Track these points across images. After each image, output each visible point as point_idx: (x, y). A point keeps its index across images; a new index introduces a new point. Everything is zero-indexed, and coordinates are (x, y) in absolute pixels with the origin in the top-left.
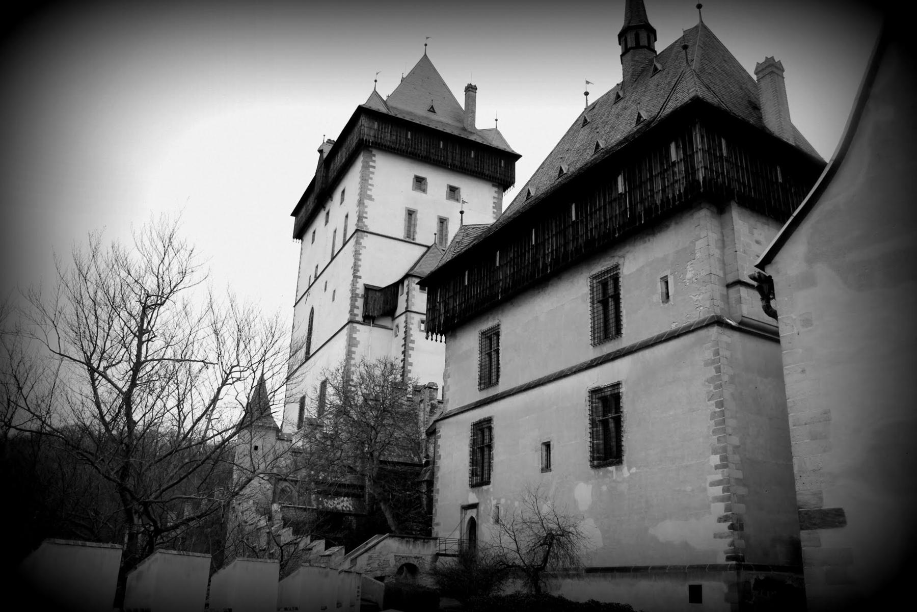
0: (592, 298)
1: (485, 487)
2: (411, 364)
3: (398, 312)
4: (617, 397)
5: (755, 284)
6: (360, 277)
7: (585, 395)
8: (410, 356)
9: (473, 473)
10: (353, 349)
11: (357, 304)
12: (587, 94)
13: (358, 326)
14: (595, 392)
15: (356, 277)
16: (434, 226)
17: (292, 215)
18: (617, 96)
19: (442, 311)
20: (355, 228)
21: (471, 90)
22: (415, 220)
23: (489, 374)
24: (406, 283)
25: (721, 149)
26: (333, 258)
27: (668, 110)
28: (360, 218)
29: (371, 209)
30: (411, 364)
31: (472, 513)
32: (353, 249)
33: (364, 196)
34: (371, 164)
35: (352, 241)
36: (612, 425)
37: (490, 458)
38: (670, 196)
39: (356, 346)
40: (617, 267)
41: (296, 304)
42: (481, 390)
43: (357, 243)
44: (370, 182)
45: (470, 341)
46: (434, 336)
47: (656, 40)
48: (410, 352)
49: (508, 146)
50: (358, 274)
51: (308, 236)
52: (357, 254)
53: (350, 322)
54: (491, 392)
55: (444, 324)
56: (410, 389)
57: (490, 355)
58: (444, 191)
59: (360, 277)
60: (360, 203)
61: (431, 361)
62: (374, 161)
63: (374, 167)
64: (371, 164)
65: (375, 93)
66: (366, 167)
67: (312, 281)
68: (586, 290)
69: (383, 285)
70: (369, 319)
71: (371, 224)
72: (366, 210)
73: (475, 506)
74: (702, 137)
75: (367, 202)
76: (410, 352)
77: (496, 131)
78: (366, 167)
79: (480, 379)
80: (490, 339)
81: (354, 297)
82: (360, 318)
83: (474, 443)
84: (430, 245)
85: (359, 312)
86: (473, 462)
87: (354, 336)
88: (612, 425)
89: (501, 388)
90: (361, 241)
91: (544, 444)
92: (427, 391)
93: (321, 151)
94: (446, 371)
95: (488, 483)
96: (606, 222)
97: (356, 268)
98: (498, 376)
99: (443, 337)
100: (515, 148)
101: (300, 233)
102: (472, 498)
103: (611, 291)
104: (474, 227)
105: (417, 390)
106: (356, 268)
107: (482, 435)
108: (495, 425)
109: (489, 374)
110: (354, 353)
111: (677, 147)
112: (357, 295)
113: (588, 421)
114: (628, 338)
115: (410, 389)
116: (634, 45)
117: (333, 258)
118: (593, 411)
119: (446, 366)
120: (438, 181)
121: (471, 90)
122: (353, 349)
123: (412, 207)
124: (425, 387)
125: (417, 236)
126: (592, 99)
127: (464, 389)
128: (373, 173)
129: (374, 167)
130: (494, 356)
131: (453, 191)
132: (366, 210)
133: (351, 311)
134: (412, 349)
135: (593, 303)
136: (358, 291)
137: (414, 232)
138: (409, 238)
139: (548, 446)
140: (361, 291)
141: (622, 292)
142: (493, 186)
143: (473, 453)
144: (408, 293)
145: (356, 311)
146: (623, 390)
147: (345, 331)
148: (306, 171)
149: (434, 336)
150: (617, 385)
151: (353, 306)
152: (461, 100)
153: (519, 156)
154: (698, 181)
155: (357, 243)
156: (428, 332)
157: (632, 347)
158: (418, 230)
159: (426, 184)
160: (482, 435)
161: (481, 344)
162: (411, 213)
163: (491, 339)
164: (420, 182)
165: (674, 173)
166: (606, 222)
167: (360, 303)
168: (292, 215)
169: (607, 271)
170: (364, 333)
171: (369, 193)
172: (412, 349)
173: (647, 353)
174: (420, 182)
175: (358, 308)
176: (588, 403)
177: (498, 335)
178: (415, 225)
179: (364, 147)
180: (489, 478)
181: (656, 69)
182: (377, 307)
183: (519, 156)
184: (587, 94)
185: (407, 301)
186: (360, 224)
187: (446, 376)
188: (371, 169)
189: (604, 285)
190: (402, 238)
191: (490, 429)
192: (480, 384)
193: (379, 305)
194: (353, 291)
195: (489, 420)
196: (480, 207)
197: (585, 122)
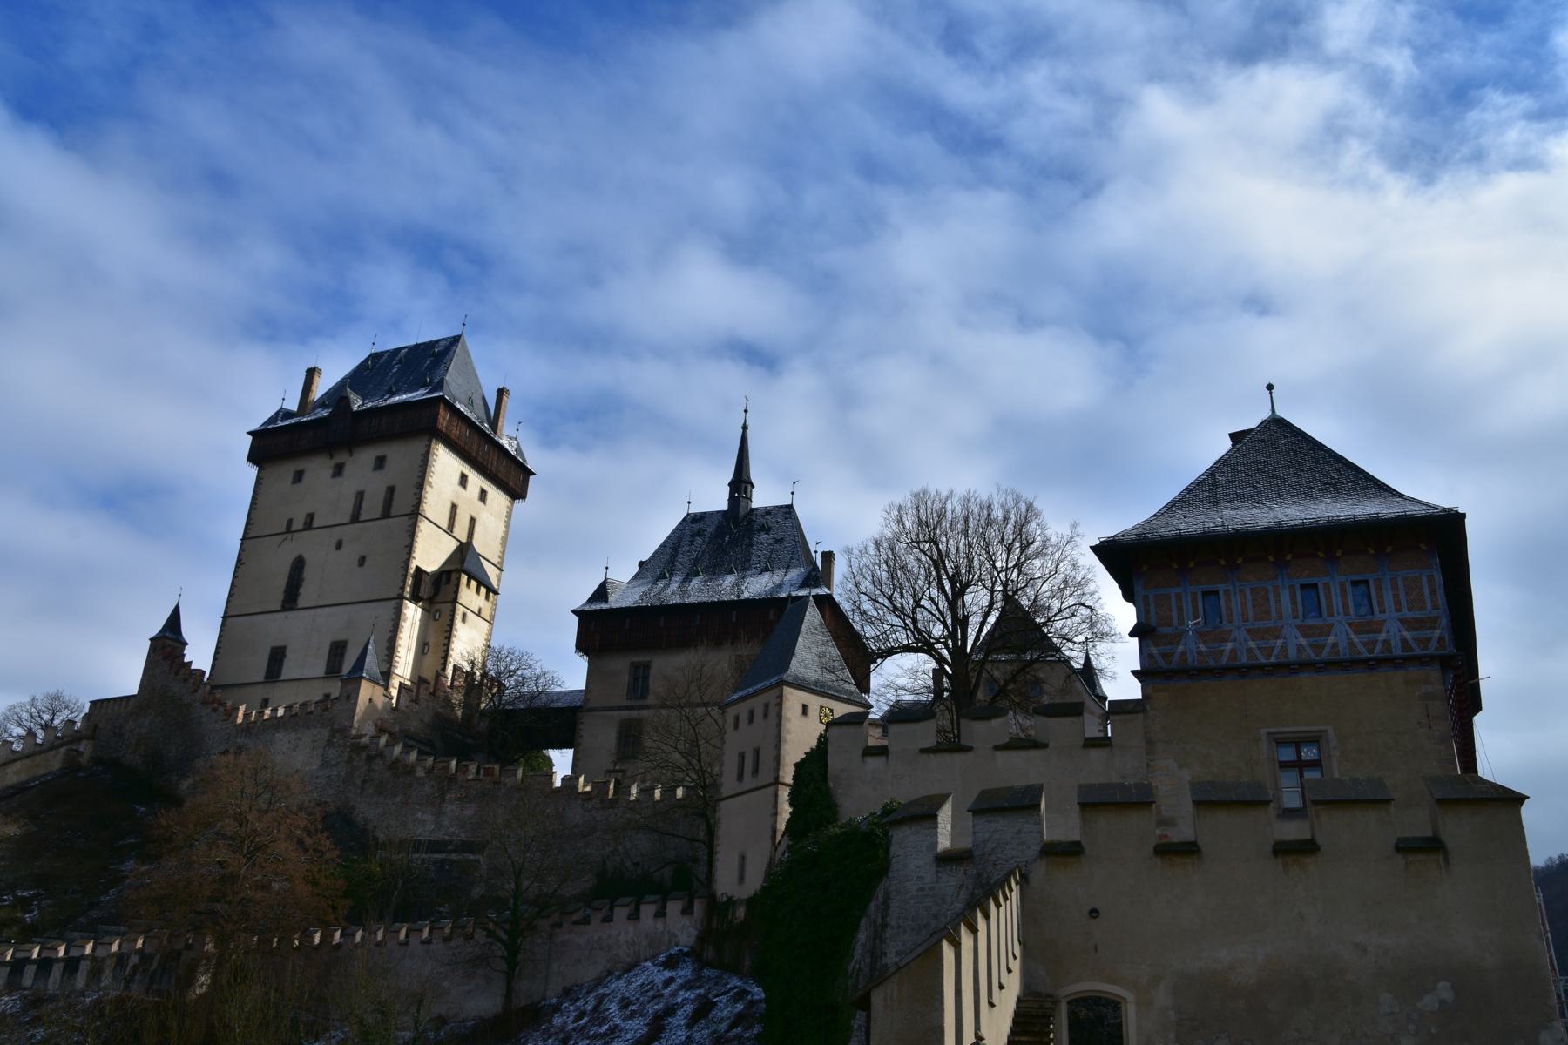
3: (439, 598)
24: (454, 576)
26: (355, 519)
58: (477, 493)
67: (298, 524)
75: (428, 488)
106: (410, 548)
120: (476, 481)
126: (696, 509)
138: (450, 529)
140: (412, 571)
155: (414, 525)
162: (454, 507)
164: (463, 480)
174: (463, 480)
179: (435, 434)
182: (425, 590)
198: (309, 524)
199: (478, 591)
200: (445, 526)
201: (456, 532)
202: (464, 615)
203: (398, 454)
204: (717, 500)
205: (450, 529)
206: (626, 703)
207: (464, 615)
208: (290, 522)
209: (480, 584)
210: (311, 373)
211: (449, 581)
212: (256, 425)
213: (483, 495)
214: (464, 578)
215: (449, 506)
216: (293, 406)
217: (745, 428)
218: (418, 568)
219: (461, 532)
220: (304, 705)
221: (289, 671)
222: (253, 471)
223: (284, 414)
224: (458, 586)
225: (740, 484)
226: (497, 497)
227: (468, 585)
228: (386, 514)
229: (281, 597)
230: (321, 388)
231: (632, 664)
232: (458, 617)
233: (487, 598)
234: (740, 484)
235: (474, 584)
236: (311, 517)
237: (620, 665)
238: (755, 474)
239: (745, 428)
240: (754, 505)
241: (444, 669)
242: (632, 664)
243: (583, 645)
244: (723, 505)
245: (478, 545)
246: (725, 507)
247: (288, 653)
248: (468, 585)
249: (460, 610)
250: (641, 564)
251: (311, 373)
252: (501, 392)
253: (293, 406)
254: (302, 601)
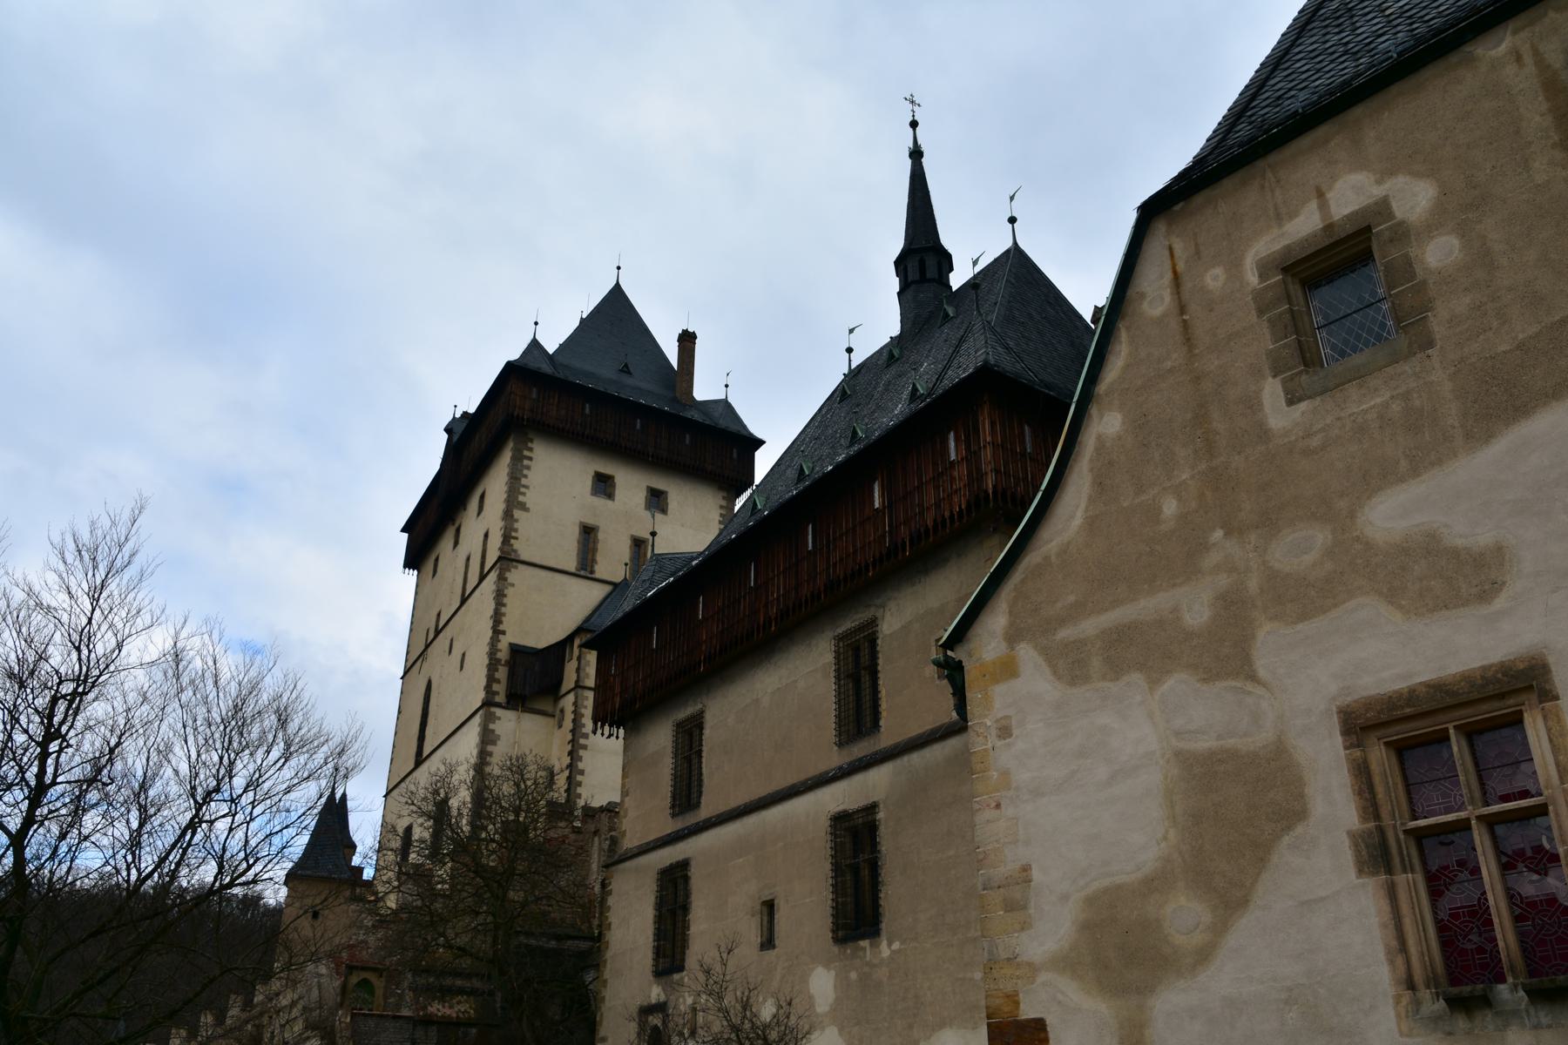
0: (837, 671)
1: (676, 977)
2: (582, 773)
3: (564, 689)
4: (873, 828)
5: (338, 796)
6: (504, 633)
7: (825, 823)
8: (580, 759)
9: (658, 953)
10: (490, 748)
11: (497, 675)
12: (849, 350)
13: (499, 712)
14: (840, 820)
15: (497, 632)
16: (624, 551)
18: (891, 355)
19: (617, 690)
20: (498, 554)
21: (687, 340)
22: (596, 541)
23: (686, 792)
25: (1023, 442)
26: (464, 600)
27: (947, 383)
28: (507, 538)
29: (523, 522)
30: (582, 773)
31: (655, 1020)
32: (494, 587)
33: (514, 503)
34: (526, 453)
35: (493, 576)
36: (865, 873)
37: (686, 927)
38: (947, 514)
39: (494, 743)
40: (873, 622)
41: (406, 673)
42: (674, 815)
43: (501, 578)
44: (524, 481)
45: (660, 738)
46: (607, 728)
47: (951, 269)
48: (581, 752)
49: (744, 427)
50: (501, 627)
52: (500, 597)
53: (487, 703)
54: (691, 819)
55: (622, 710)
56: (578, 813)
57: (689, 760)
58: (640, 497)
59: (504, 633)
60: (508, 515)
61: (604, 768)
62: (531, 450)
63: (530, 459)
64: (526, 453)
65: (535, 345)
66: (518, 459)
67: (431, 636)
68: (829, 657)
69: (542, 645)
70: (518, 700)
71: (524, 549)
72: (516, 525)
73: (660, 1008)
74: (993, 424)
75: (517, 513)
76: (581, 752)
77: (725, 405)
78: (518, 459)
79: (674, 797)
80: (691, 735)
81: (493, 665)
82: (500, 698)
83: (659, 905)
84: (618, 578)
85: (500, 688)
86: (659, 935)
87: (491, 726)
88: (865, 873)
89: (705, 811)
90: (507, 575)
91: (764, 903)
92: (604, 817)
93: (448, 430)
94: (623, 785)
95: (681, 969)
96: (855, 552)
97: (497, 618)
98: (700, 793)
99: (622, 731)
100: (756, 430)
101: (415, 558)
102: (656, 993)
103: (865, 659)
104: (672, 557)
105: (590, 813)
107: (674, 889)
108: (695, 873)
109: (686, 792)
110: (491, 754)
111: (957, 440)
112: (499, 661)
113: (828, 866)
114: (888, 737)
115: (578, 813)
116: (917, 277)
117: (464, 600)
118: (837, 850)
119: (624, 776)
121: (687, 340)
122: (490, 748)
123: (590, 521)
124: (602, 809)
125: (597, 568)
126: (858, 359)
127: (646, 817)
128: (528, 468)
129: (530, 459)
130: (695, 761)
131: (657, 500)
132: (516, 525)
133: (488, 688)
134: (585, 747)
135: (838, 678)
136: (499, 655)
137: (594, 561)
139: (770, 906)
140: (503, 655)
141: (880, 661)
142: (721, 488)
143: (659, 919)
144: (579, 659)
145: (496, 687)
146: (881, 815)
147: (477, 719)
148: (425, 460)
149: (607, 728)
150: (872, 808)
151: (491, 679)
152: (672, 353)
153: (761, 443)
154: (986, 491)
156: (595, 723)
157: (896, 746)
158: (599, 558)
159: (613, 486)
160: (674, 889)
161: (676, 742)
162: (588, 533)
163: (690, 738)
164: (604, 485)
165: (953, 479)
166: (855, 552)
167: (502, 674)
169: (860, 629)
170: (507, 723)
171: (521, 498)
172: (585, 747)
173: (915, 758)
174: (604, 485)
175: (498, 681)
176: (829, 837)
177: (701, 727)
178: (595, 550)
180: (683, 960)
181: (947, 315)
183: (761, 443)
184: (849, 350)
185: (578, 670)
186: (506, 548)
187: (625, 793)
188: (526, 462)
189: (856, 650)
190: (573, 570)
191: (686, 879)
192: (673, 807)
193: (528, 678)
194: (492, 653)
195: (684, 865)
196: (692, 525)
197: (844, 392)
200: (572, 566)
201: (601, 571)
205: (585, 568)
206: (670, 826)
215: (574, 534)
217: (916, 154)
218: (516, 650)
222: (411, 577)
228: (482, 578)
239: (916, 154)
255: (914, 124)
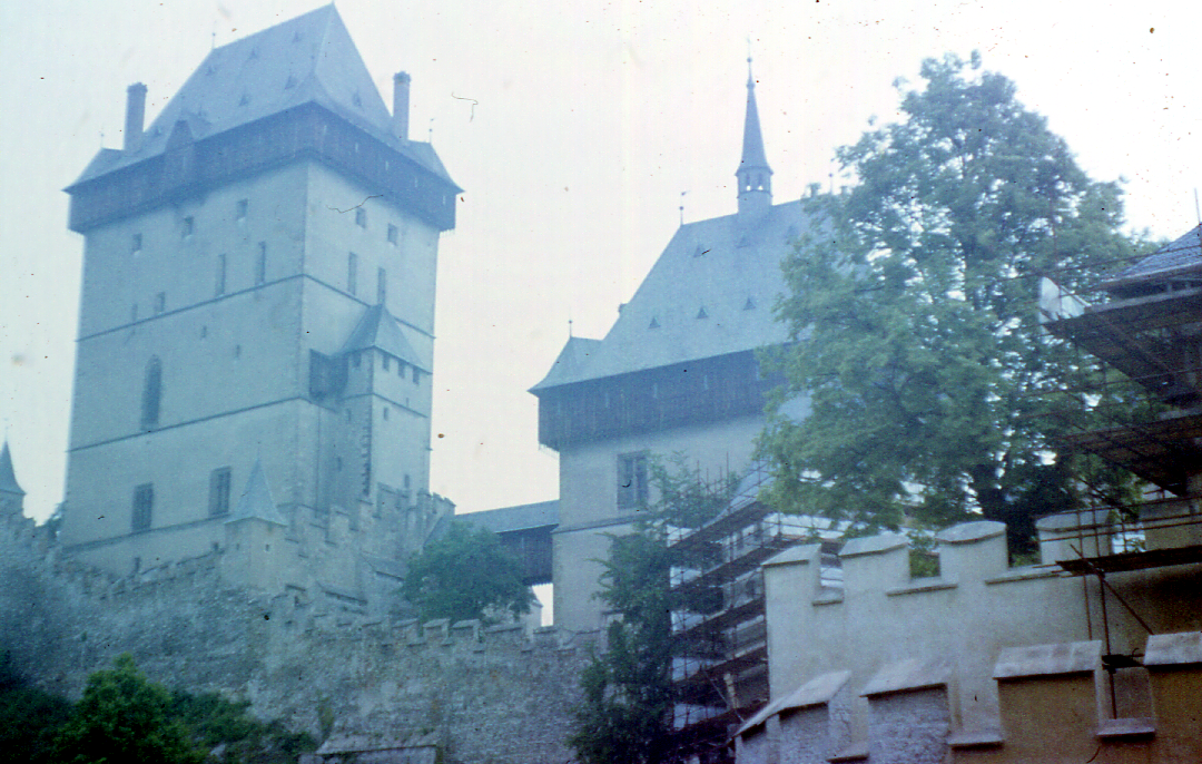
17: (66, 190)
21: (402, 80)
24: (364, 358)
51: (118, 237)
67: (146, 312)
77: (428, 147)
100: (456, 178)
120: (380, 216)
138: (350, 294)
140: (305, 354)
153: (461, 191)
164: (360, 218)
168: (66, 190)
174: (360, 218)
179: (307, 155)
183: (461, 191)
198: (161, 312)
199: (401, 373)
200: (344, 287)
202: (386, 410)
203: (266, 190)
204: (726, 203)
207: (386, 410)
208: (135, 308)
209: (402, 363)
210: (137, 93)
211: (358, 364)
212: (72, 178)
213: (391, 230)
214: (378, 362)
216: (117, 143)
217: (750, 86)
218: (314, 355)
219: (368, 291)
220: (183, 563)
221: (161, 517)
222: (78, 242)
223: (107, 155)
224: (371, 370)
225: (754, 171)
226: (414, 234)
227: (386, 367)
229: (136, 415)
230: (151, 114)
231: (620, 456)
232: (378, 419)
233: (416, 380)
234: (754, 171)
235: (394, 365)
236: (162, 297)
237: (603, 463)
238: (772, 155)
240: (775, 202)
241: (366, 492)
242: (620, 456)
243: (550, 437)
244: (730, 207)
245: (392, 307)
246: (730, 207)
247: (156, 489)
248: (386, 367)
249: (378, 406)
250: (622, 307)
251: (137, 93)
252: (402, 80)
253: (117, 143)
254: (164, 420)
255: (749, 60)
